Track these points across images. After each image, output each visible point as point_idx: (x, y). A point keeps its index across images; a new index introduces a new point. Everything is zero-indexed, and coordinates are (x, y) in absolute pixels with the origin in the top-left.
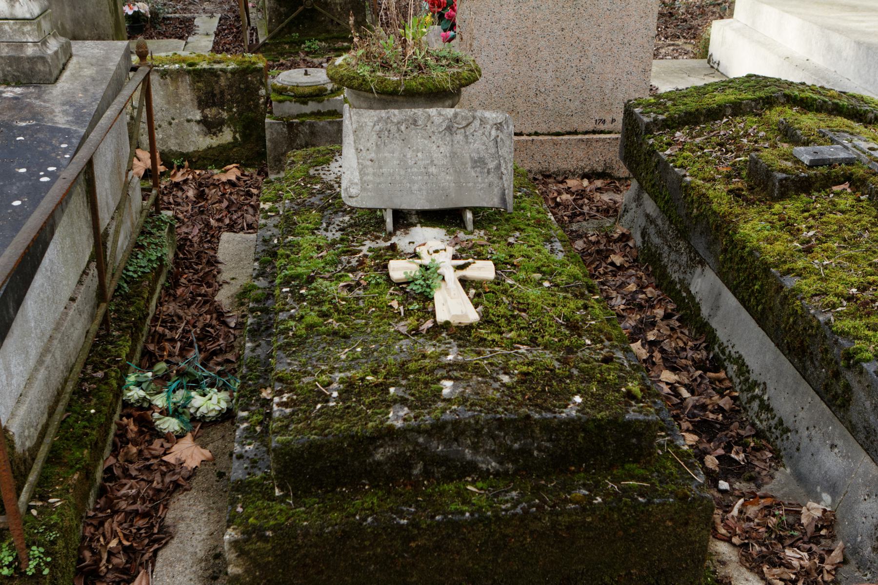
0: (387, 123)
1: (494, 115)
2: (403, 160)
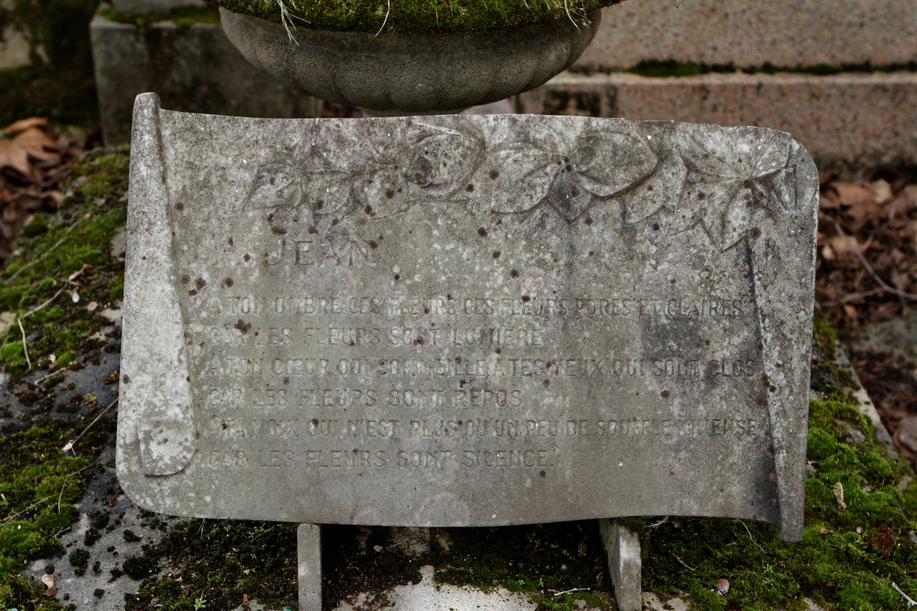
0: (308, 176)
1: (744, 147)
2: (369, 329)
